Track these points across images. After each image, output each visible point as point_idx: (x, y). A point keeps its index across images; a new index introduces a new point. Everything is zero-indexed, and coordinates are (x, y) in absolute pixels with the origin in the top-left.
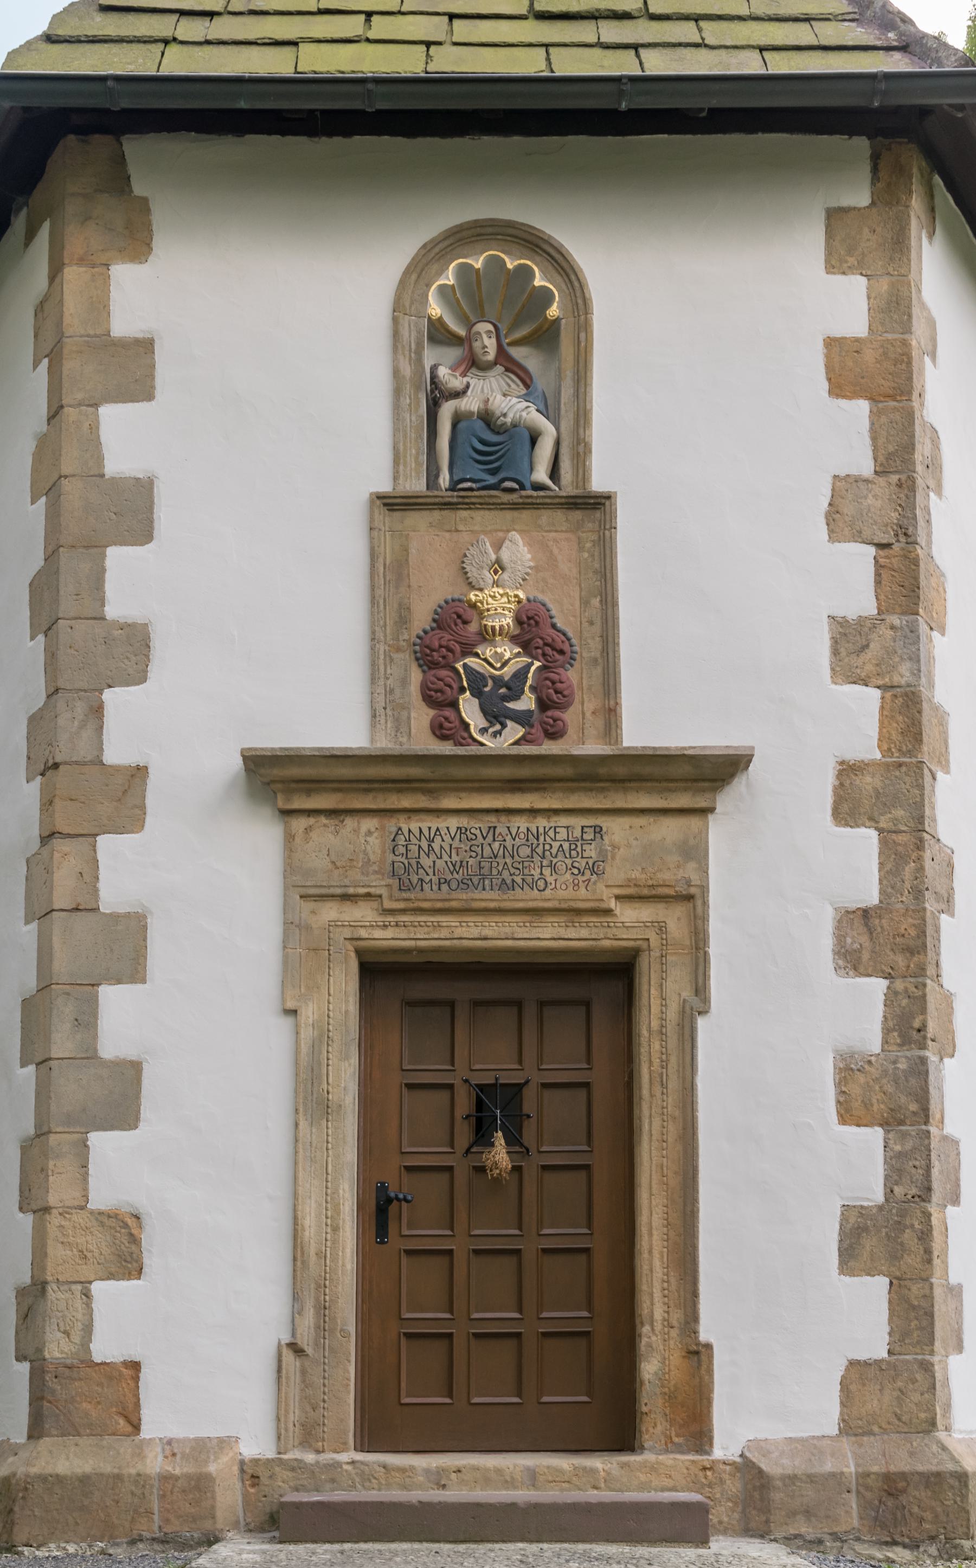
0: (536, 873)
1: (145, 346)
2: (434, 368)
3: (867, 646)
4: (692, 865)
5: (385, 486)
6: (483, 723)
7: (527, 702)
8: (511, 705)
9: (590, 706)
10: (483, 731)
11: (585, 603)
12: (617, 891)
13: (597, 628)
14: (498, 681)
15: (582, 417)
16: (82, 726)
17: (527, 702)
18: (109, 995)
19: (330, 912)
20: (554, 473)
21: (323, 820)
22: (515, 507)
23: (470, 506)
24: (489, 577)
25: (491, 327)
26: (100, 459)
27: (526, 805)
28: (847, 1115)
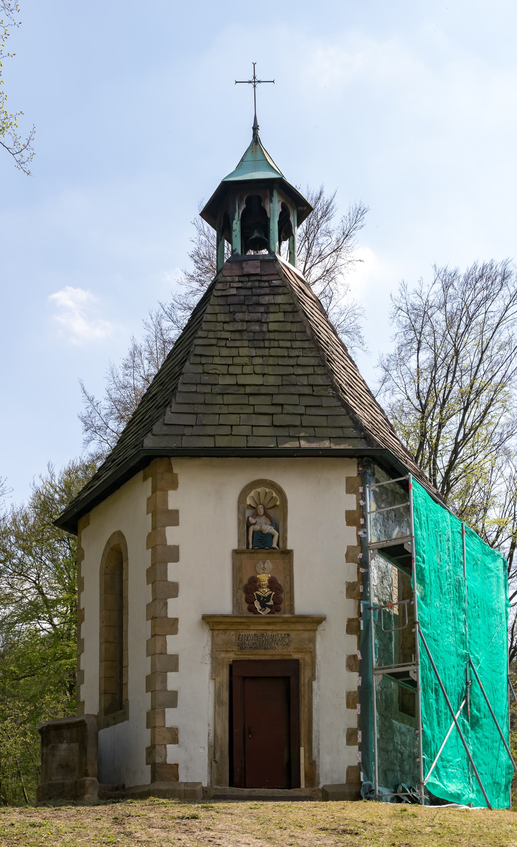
0: (273, 645)
1: (177, 512)
2: (248, 517)
3: (355, 589)
4: (311, 644)
5: (236, 547)
6: (260, 608)
7: (271, 603)
8: (267, 603)
9: (287, 604)
10: (260, 610)
11: (285, 577)
12: (293, 650)
13: (288, 584)
14: (264, 597)
15: (285, 531)
16: (162, 608)
17: (271, 603)
19: (223, 655)
20: (278, 545)
21: (221, 632)
22: (269, 553)
23: (257, 553)
24: (262, 571)
25: (262, 506)
26: (166, 540)
27: (271, 629)
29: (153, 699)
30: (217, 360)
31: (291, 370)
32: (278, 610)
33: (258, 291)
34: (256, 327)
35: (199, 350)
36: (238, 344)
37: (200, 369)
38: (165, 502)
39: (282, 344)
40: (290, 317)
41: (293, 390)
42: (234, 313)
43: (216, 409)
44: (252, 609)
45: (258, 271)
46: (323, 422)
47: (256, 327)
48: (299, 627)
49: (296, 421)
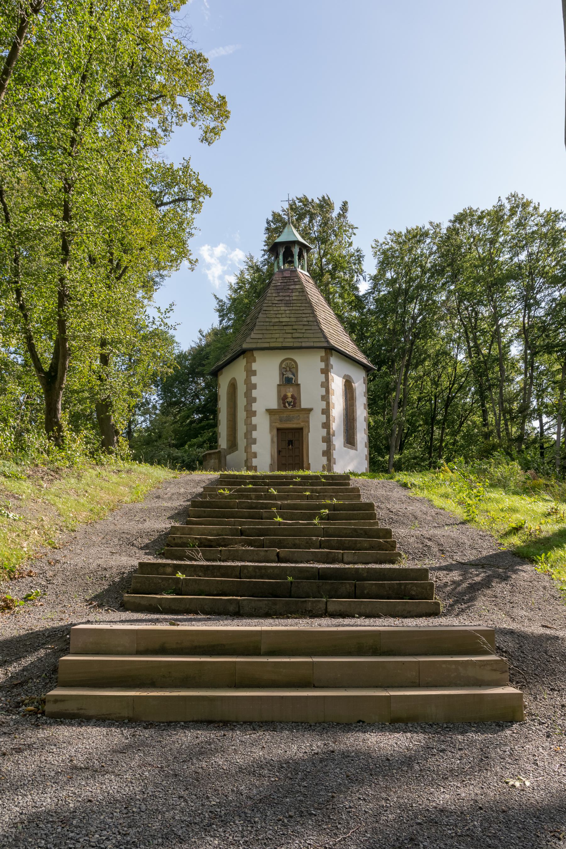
7: (292, 404)
17: (292, 404)
18: (253, 432)
19: (274, 424)
28: (323, 442)
29: (247, 442)
30: (272, 312)
31: (301, 315)
32: (295, 407)
33: (289, 284)
34: (287, 298)
35: (265, 308)
36: (280, 305)
37: (265, 316)
38: (251, 367)
39: (297, 305)
40: (301, 294)
41: (301, 323)
42: (279, 293)
43: (271, 332)
44: (285, 407)
45: (289, 275)
46: (311, 335)
47: (287, 298)
48: (303, 412)
49: (301, 335)
